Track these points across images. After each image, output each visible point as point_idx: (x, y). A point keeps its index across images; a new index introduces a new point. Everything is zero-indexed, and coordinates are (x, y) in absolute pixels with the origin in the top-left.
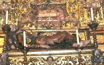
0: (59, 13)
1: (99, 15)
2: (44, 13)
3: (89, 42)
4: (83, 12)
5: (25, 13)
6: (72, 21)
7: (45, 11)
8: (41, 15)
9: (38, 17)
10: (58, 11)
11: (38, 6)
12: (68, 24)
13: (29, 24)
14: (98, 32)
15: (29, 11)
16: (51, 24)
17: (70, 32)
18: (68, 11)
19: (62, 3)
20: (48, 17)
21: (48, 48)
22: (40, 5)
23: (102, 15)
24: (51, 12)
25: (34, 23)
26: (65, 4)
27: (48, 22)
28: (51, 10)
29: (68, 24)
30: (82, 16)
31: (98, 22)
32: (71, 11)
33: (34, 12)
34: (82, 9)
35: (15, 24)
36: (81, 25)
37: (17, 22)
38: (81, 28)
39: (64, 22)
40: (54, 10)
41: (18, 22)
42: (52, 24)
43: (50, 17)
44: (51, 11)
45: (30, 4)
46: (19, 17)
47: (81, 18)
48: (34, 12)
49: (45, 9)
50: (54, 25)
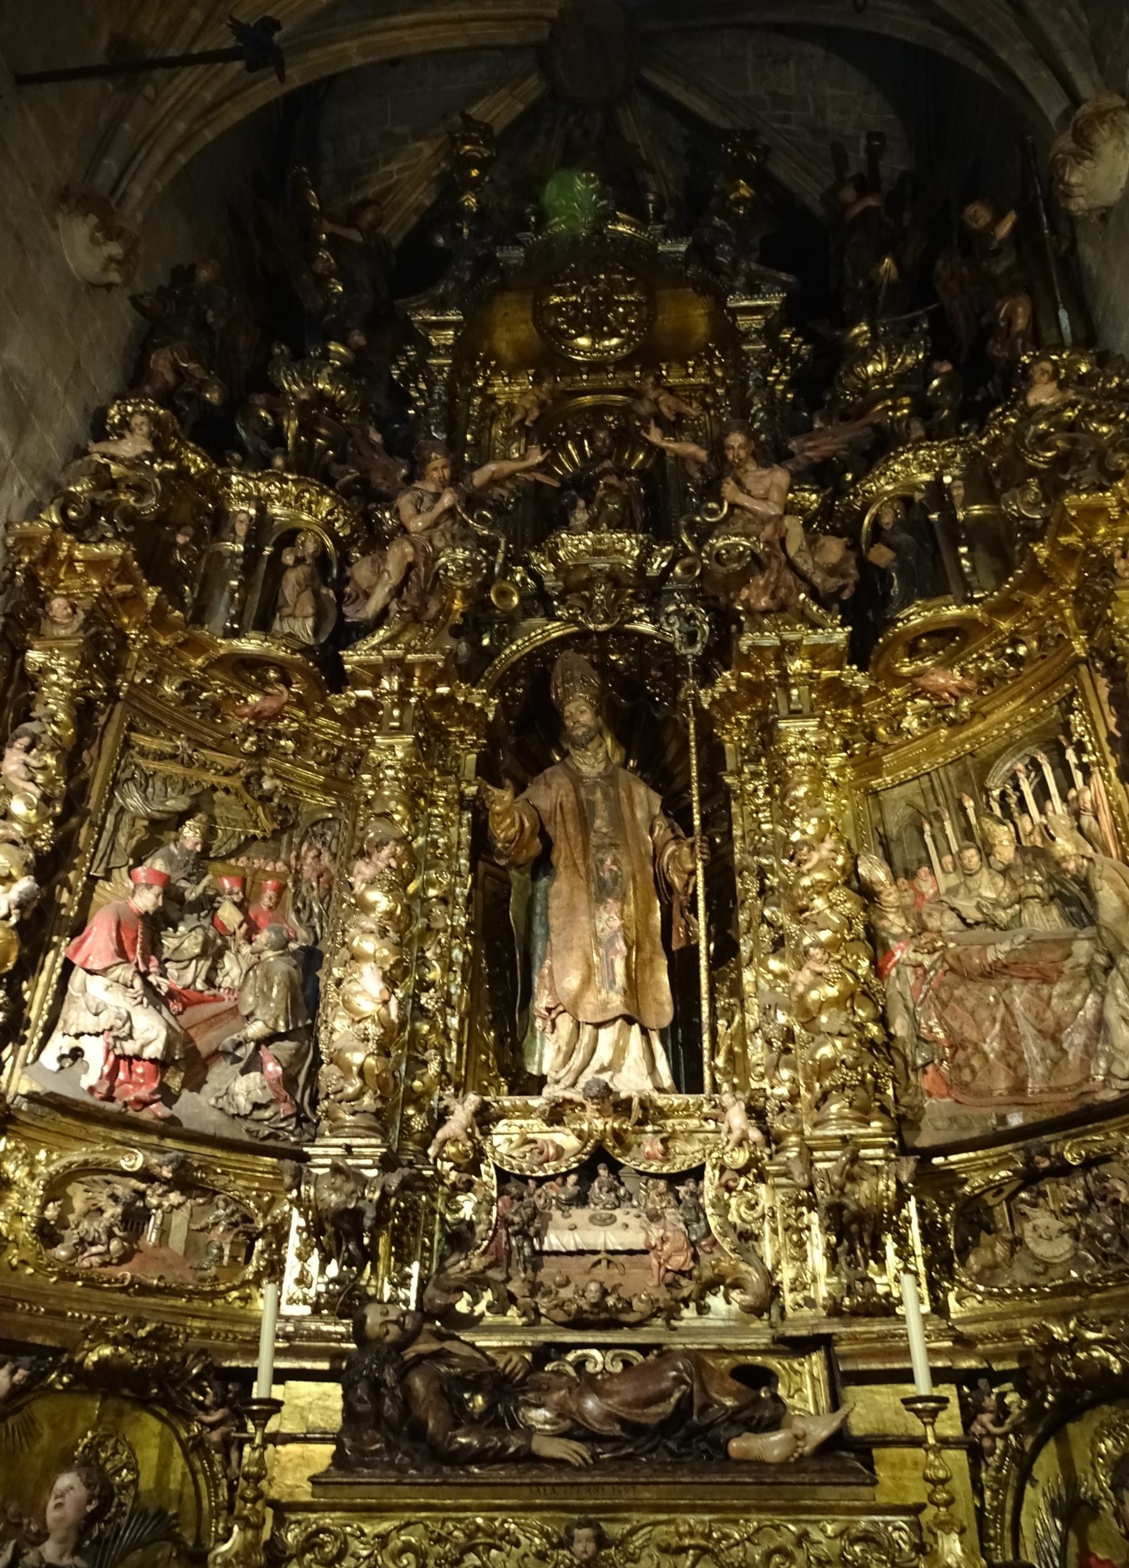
0: (656, 1232)
1: (898, 1253)
2: (573, 1228)
3: (835, 1424)
4: (800, 1231)
5: (464, 1227)
6: (737, 1285)
7: (580, 1215)
8: (553, 1240)
9: (542, 1253)
10: (655, 1217)
11: (540, 1181)
12: (716, 1302)
13: (488, 1296)
14: (888, 1366)
15: (489, 1213)
16: (610, 1301)
17: (721, 1351)
18: (713, 1222)
19: (679, 1165)
20: (595, 1252)
21: (576, 1460)
22: (552, 1178)
23: (919, 1249)
24: (613, 1219)
25: (513, 1287)
26: (697, 1173)
27: (593, 1287)
28: (615, 1207)
29: (716, 1302)
30: (794, 1258)
31: (888, 1295)
32: (733, 1217)
33: (517, 1219)
34: (792, 1211)
35: (402, 1293)
36: (789, 1312)
37: (414, 1283)
38: (791, 1332)
39: (688, 1287)
40: (634, 1212)
41: (421, 1279)
42: (619, 1299)
43: (609, 1252)
44: (617, 1212)
45: (493, 1171)
46: (430, 1250)
47: (784, 1264)
48: (513, 1223)
49: (581, 1199)
50: (630, 1304)
